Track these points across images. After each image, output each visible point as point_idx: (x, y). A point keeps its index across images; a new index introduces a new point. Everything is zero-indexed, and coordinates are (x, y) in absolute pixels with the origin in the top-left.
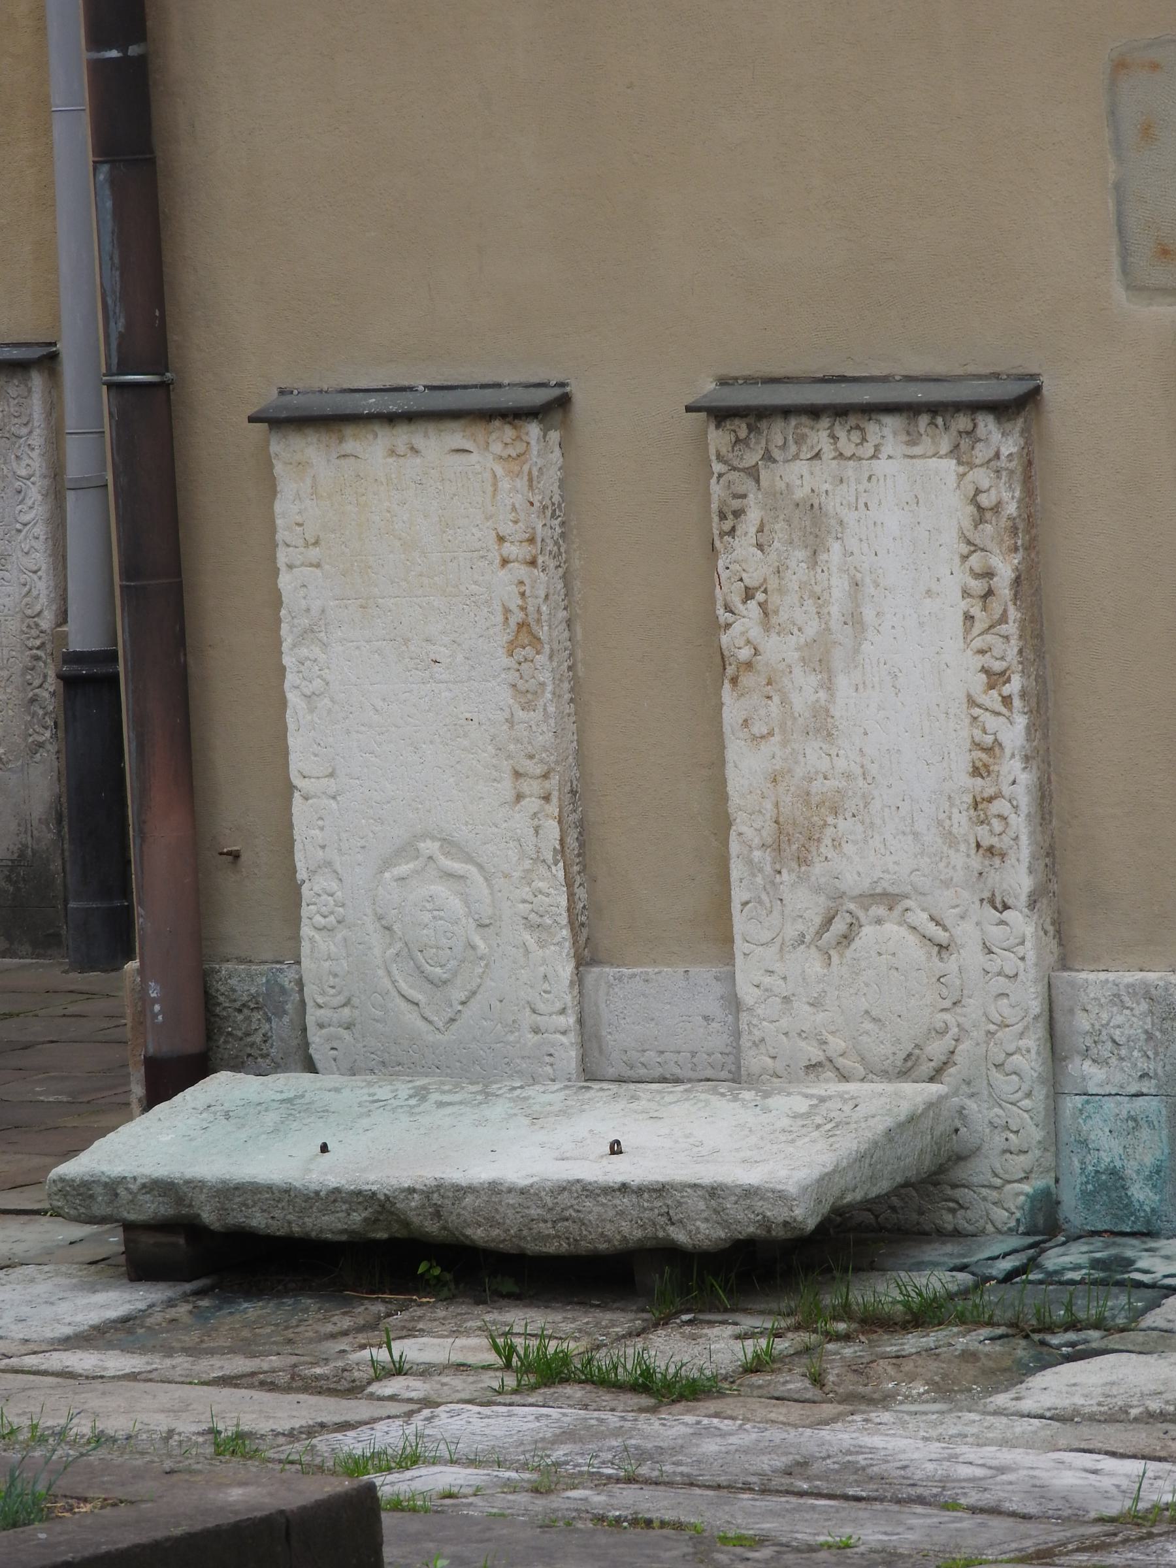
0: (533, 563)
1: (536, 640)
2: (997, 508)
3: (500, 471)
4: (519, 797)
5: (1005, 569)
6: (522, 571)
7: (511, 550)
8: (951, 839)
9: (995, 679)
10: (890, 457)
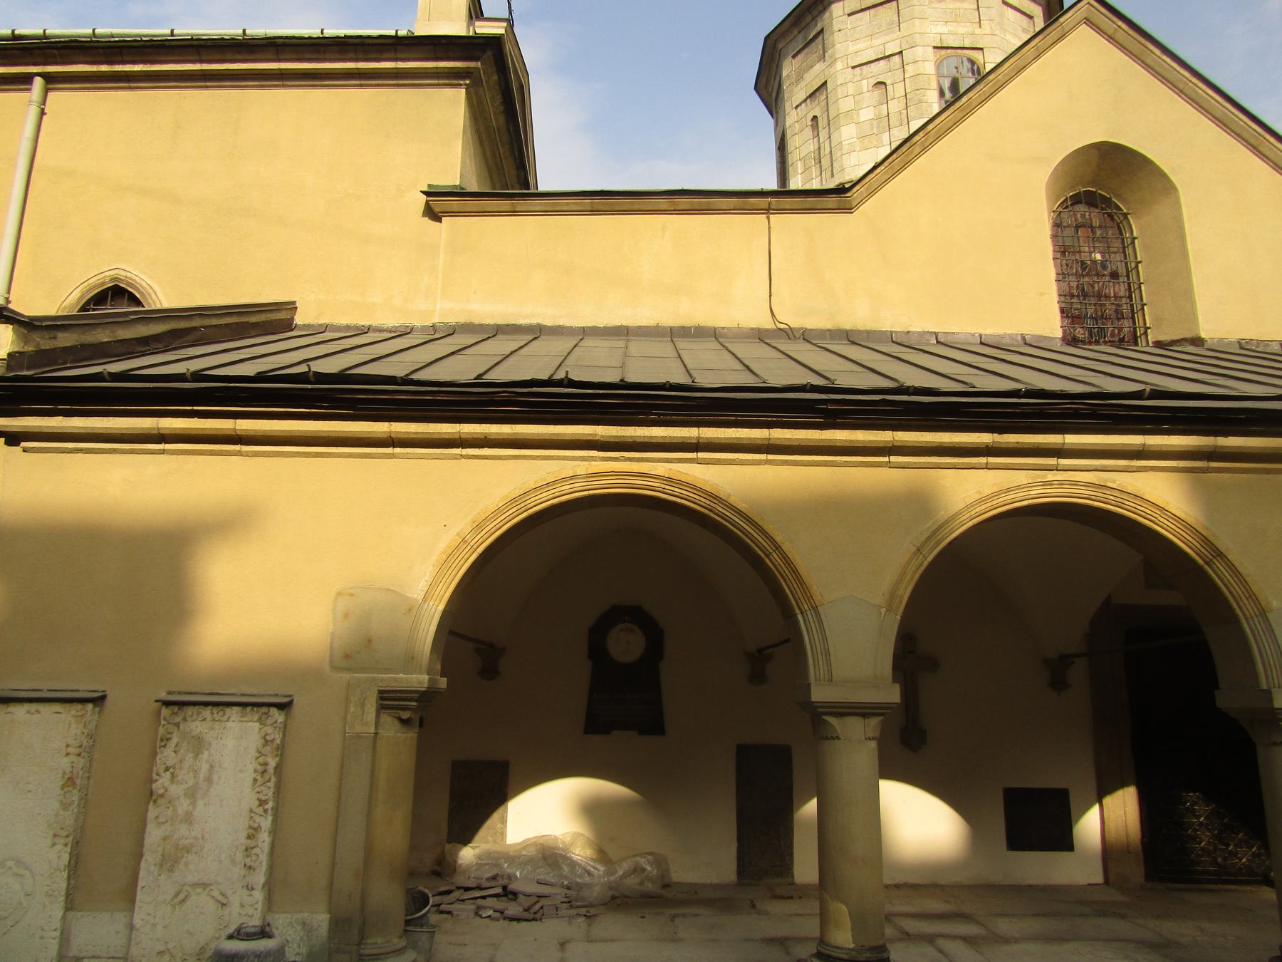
0: (79, 755)
1: (74, 784)
2: (273, 741)
3: (73, 721)
4: (54, 845)
5: (272, 763)
6: (74, 758)
7: (71, 750)
8: (233, 863)
9: (262, 803)
10: (233, 721)
